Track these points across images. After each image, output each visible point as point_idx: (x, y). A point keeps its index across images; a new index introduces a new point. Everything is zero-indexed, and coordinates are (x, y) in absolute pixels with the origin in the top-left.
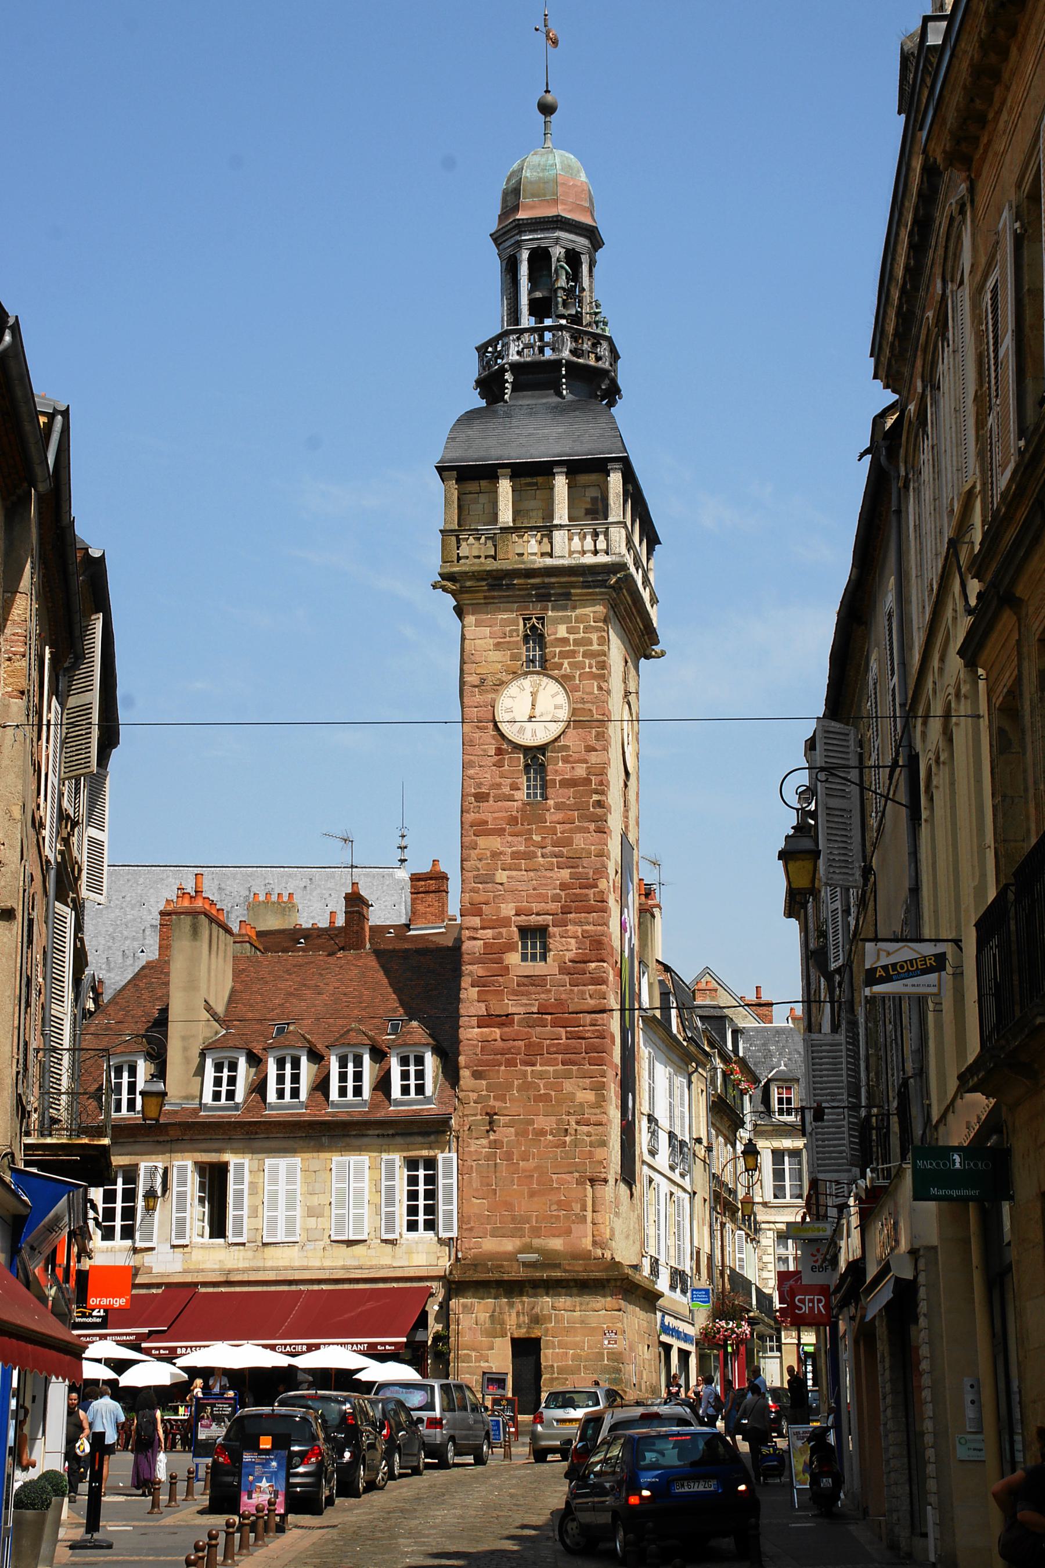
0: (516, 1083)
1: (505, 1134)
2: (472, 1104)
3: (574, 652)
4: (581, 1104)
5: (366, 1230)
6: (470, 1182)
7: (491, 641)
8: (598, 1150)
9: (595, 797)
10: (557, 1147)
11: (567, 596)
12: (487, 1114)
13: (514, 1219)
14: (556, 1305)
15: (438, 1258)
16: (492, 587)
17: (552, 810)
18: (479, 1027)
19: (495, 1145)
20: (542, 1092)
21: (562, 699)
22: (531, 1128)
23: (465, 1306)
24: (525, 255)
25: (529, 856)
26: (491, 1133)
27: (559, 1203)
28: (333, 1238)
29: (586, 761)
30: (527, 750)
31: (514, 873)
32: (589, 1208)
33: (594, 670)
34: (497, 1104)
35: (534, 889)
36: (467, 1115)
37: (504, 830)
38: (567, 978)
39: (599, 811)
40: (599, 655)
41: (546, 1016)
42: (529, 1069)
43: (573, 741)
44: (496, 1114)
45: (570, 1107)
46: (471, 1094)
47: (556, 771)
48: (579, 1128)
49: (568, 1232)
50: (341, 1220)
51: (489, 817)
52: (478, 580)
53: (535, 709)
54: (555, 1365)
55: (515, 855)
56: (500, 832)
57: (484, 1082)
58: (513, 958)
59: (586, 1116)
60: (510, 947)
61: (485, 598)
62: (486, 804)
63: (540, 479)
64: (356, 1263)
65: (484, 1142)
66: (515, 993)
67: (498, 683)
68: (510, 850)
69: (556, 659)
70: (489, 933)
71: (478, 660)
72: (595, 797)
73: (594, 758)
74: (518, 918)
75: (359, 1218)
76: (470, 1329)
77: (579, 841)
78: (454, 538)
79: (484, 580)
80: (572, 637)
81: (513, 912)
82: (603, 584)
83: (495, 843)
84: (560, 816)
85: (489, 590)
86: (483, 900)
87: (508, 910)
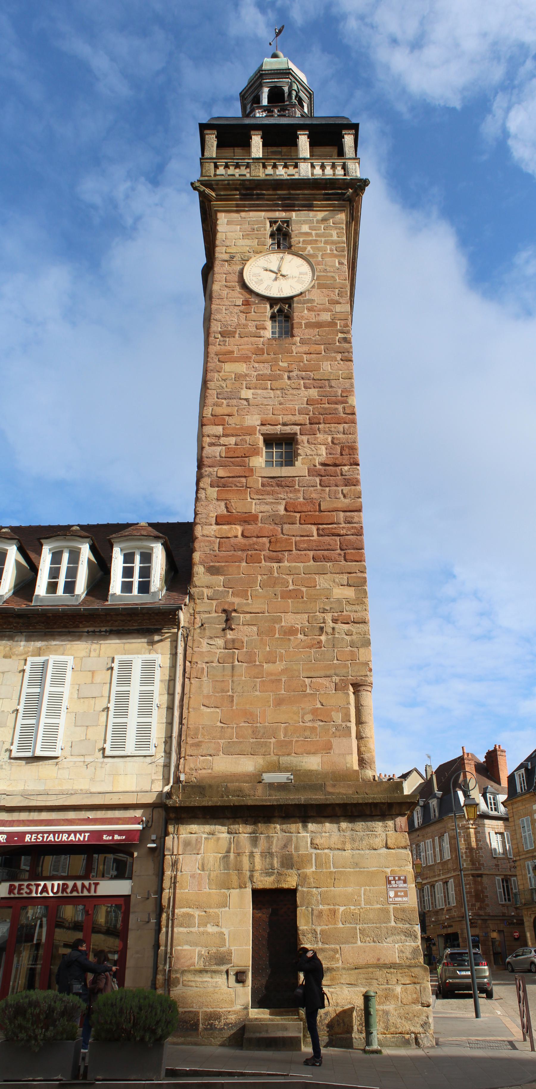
0: (259, 578)
1: (244, 632)
2: (206, 600)
3: (316, 241)
4: (339, 601)
5: (60, 744)
6: (200, 687)
7: (241, 234)
8: (362, 650)
9: (340, 335)
10: (310, 647)
11: (309, 207)
12: (224, 611)
13: (255, 732)
14: (317, 841)
15: (153, 781)
16: (244, 197)
17: (299, 344)
18: (217, 524)
19: (231, 645)
20: (291, 587)
21: (305, 268)
22: (277, 626)
23: (187, 844)
24: (266, 91)
25: (273, 378)
26: (228, 632)
27: (314, 711)
28: (14, 754)
29: (330, 311)
30: (273, 301)
31: (259, 391)
32: (353, 719)
33: (335, 252)
34: (236, 600)
35: (280, 404)
36: (199, 613)
37: (250, 358)
38: (318, 480)
39: (346, 345)
40: (339, 243)
41: (295, 514)
42: (275, 565)
43: (318, 297)
44: (235, 611)
45: (325, 603)
46: (205, 590)
47: (303, 316)
48: (336, 626)
49: (328, 748)
50: (29, 733)
51: (235, 349)
52: (232, 190)
53: (279, 275)
54: (318, 929)
55: (260, 377)
56: (245, 359)
57: (222, 578)
58: (259, 462)
59: (345, 613)
60: (256, 452)
61: (237, 206)
62: (232, 339)
63: (284, 149)
64: (41, 788)
65: (220, 642)
66: (258, 492)
67: (246, 258)
68: (256, 374)
69: (300, 245)
70: (232, 440)
71: (228, 244)
72: (340, 335)
73: (338, 308)
74: (263, 427)
75: (52, 731)
76: (193, 876)
77: (326, 367)
78: (212, 165)
79: (236, 189)
80: (314, 232)
81: (259, 423)
82: (340, 197)
83: (242, 368)
84: (305, 348)
85: (241, 199)
86: (226, 412)
87: (253, 420)
